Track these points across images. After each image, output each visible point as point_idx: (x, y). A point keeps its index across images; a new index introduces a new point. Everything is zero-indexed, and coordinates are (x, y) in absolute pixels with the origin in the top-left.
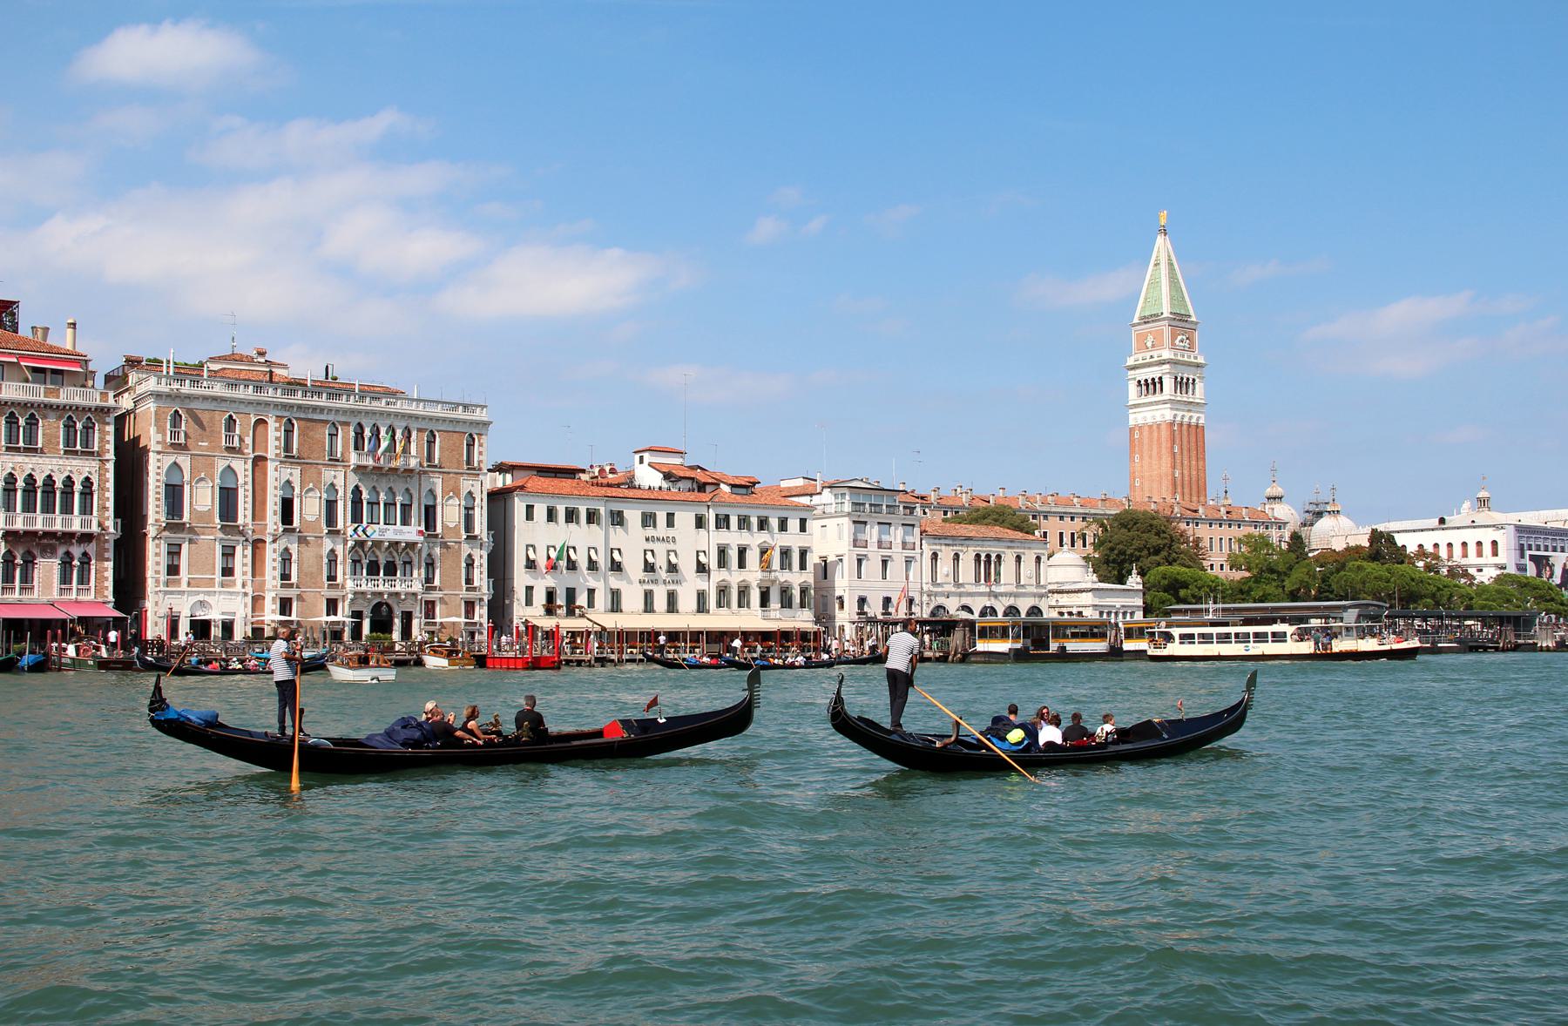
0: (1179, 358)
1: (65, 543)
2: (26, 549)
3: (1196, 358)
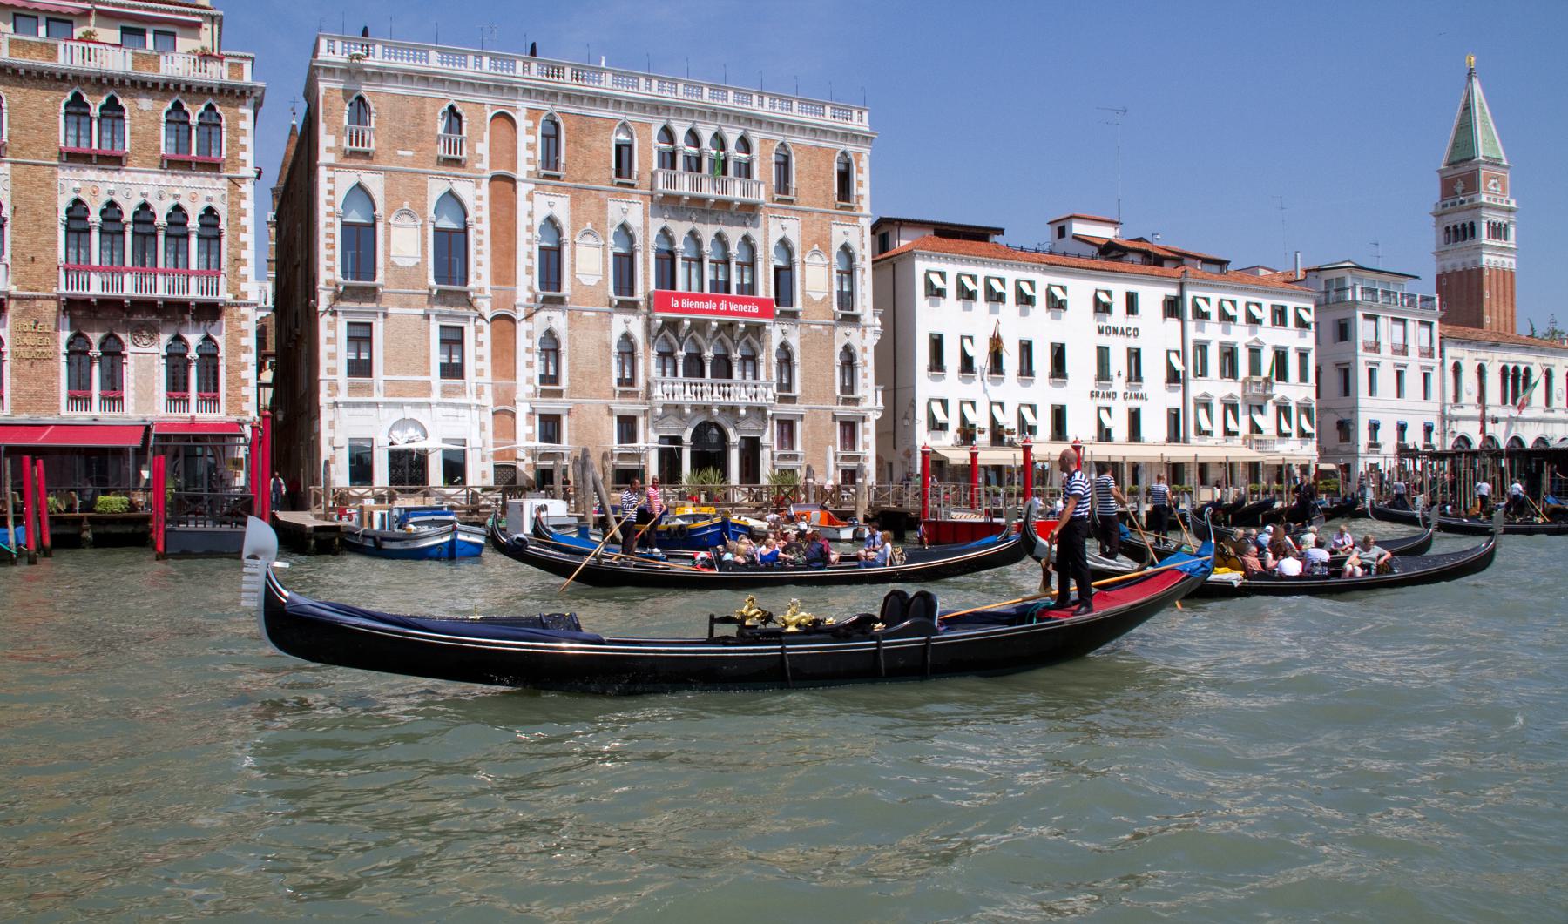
0: (1492, 202)
1: (173, 321)
3: (1508, 202)
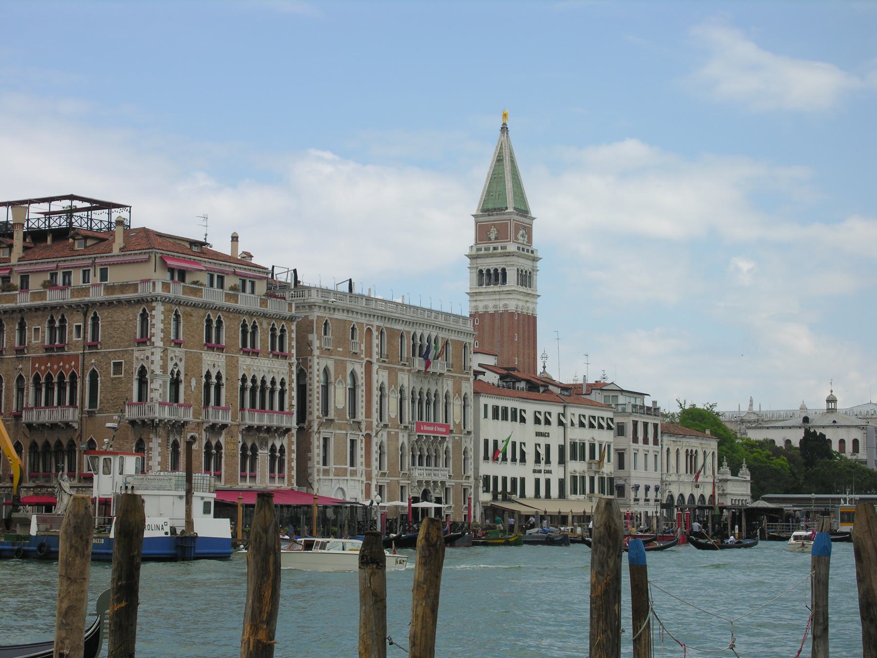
2: (252, 442)
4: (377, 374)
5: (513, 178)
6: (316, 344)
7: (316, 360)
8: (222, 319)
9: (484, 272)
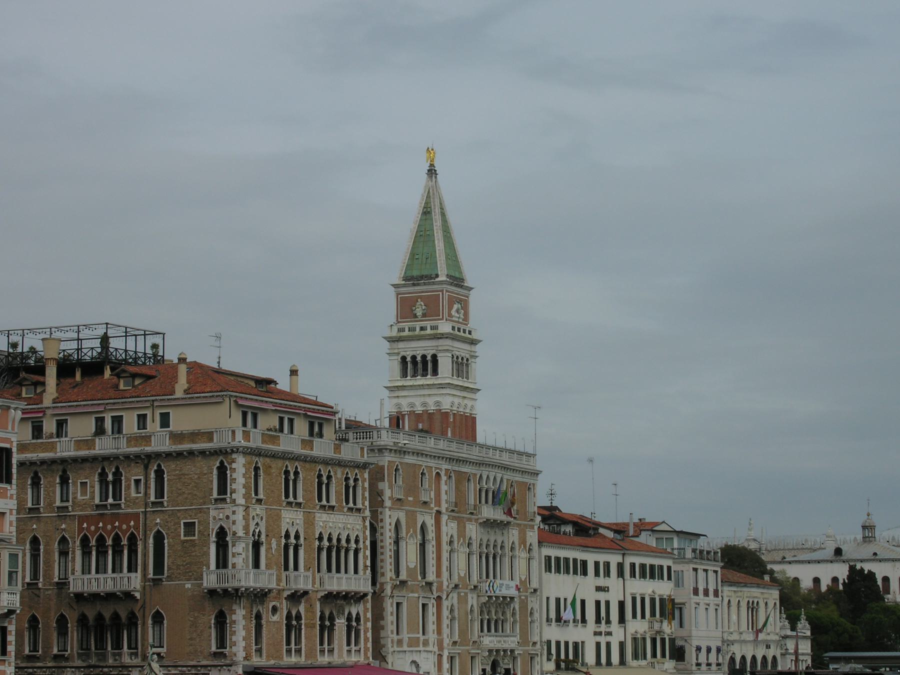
2: (330, 611)
4: (447, 525)
5: (445, 236)
6: (388, 493)
7: (387, 512)
8: (299, 470)
9: (409, 359)
